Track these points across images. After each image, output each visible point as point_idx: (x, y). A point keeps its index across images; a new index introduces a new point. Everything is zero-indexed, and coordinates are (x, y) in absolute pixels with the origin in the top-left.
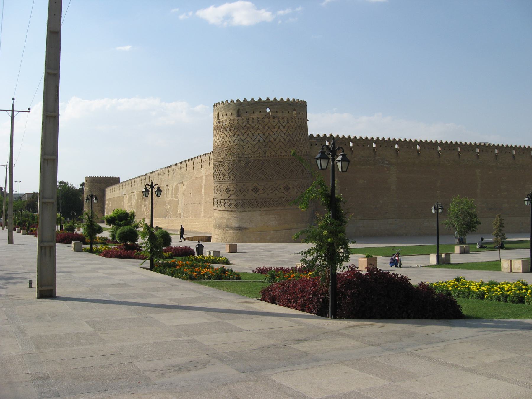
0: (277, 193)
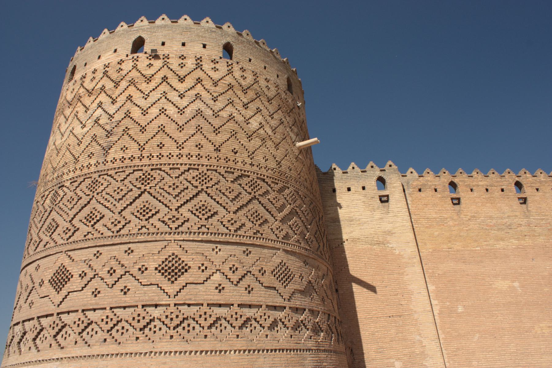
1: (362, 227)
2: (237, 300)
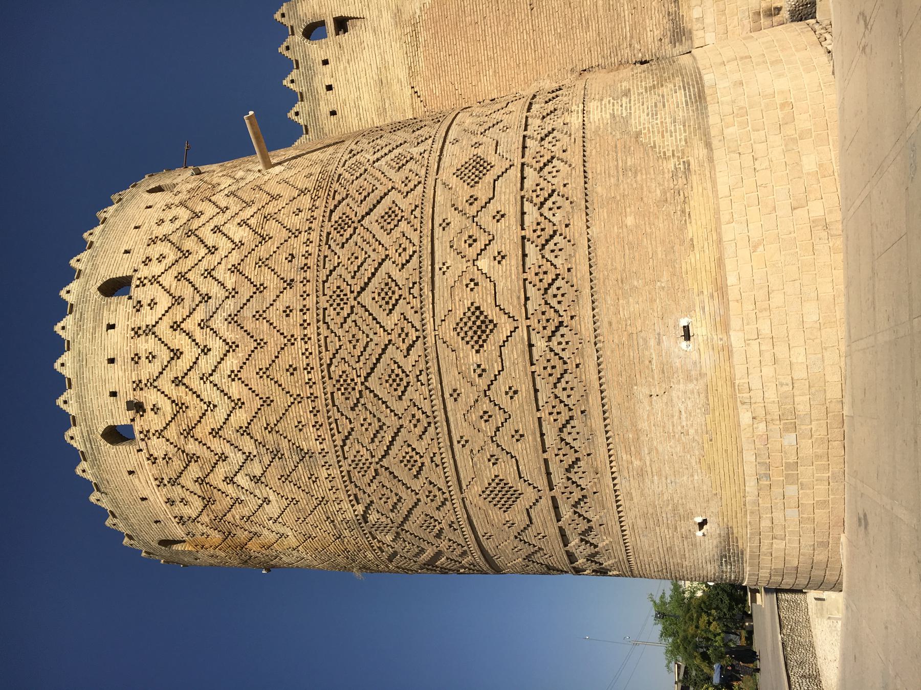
0: (504, 388)
1: (391, 63)
2: (516, 233)
